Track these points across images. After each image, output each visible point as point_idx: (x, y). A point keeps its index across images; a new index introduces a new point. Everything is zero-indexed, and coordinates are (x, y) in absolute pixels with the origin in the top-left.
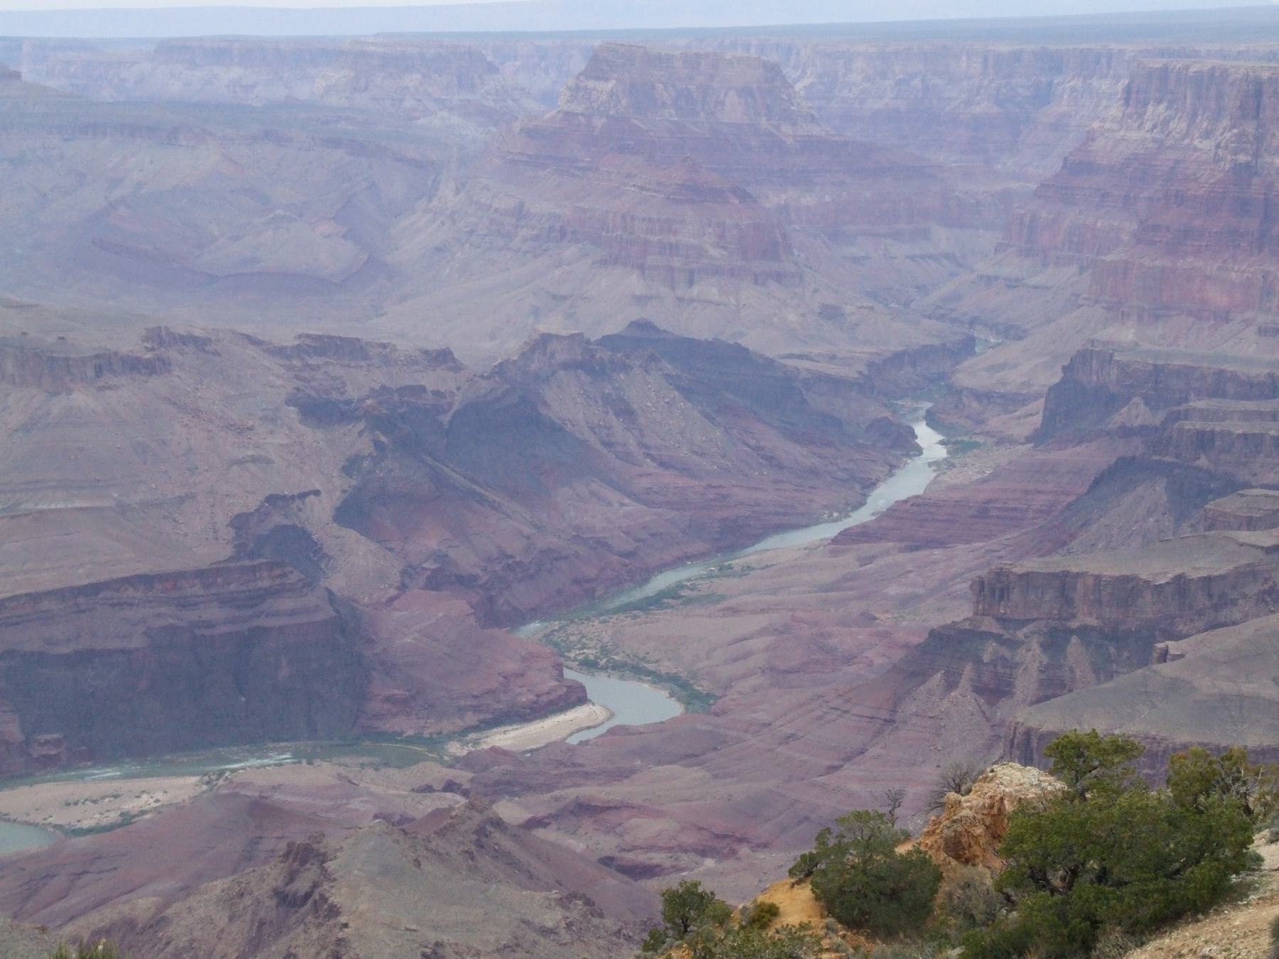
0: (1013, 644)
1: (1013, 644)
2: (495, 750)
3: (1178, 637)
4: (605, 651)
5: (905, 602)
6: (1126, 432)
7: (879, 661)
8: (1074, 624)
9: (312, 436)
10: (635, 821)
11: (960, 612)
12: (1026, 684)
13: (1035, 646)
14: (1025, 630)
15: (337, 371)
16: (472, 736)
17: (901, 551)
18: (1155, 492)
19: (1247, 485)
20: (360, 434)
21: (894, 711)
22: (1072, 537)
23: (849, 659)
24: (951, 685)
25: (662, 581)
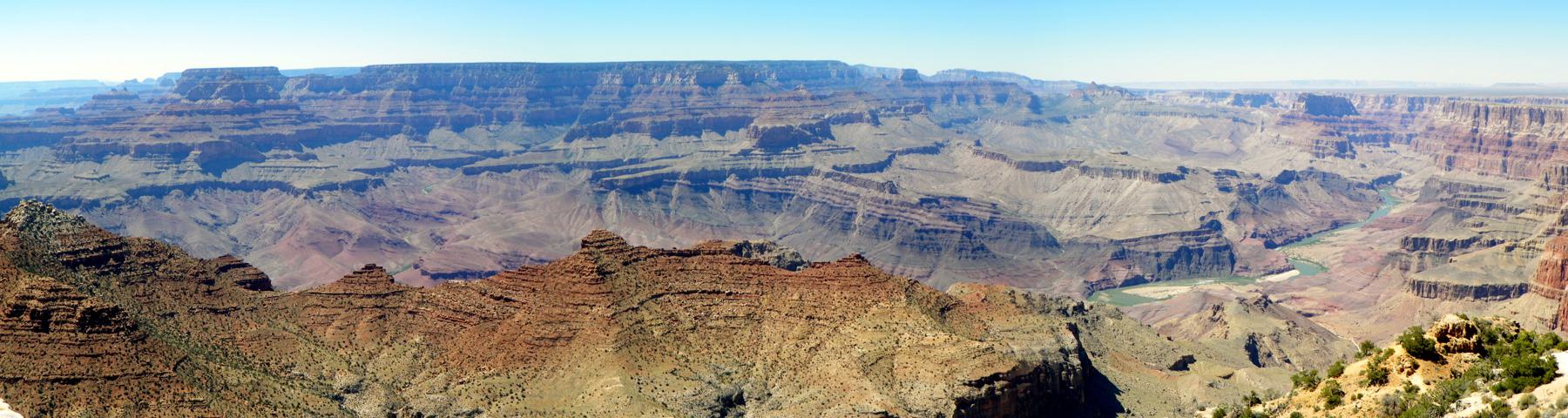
9: (1222, 195)
11: (1396, 248)
12: (1414, 268)
18: (1450, 216)
25: (1314, 237)
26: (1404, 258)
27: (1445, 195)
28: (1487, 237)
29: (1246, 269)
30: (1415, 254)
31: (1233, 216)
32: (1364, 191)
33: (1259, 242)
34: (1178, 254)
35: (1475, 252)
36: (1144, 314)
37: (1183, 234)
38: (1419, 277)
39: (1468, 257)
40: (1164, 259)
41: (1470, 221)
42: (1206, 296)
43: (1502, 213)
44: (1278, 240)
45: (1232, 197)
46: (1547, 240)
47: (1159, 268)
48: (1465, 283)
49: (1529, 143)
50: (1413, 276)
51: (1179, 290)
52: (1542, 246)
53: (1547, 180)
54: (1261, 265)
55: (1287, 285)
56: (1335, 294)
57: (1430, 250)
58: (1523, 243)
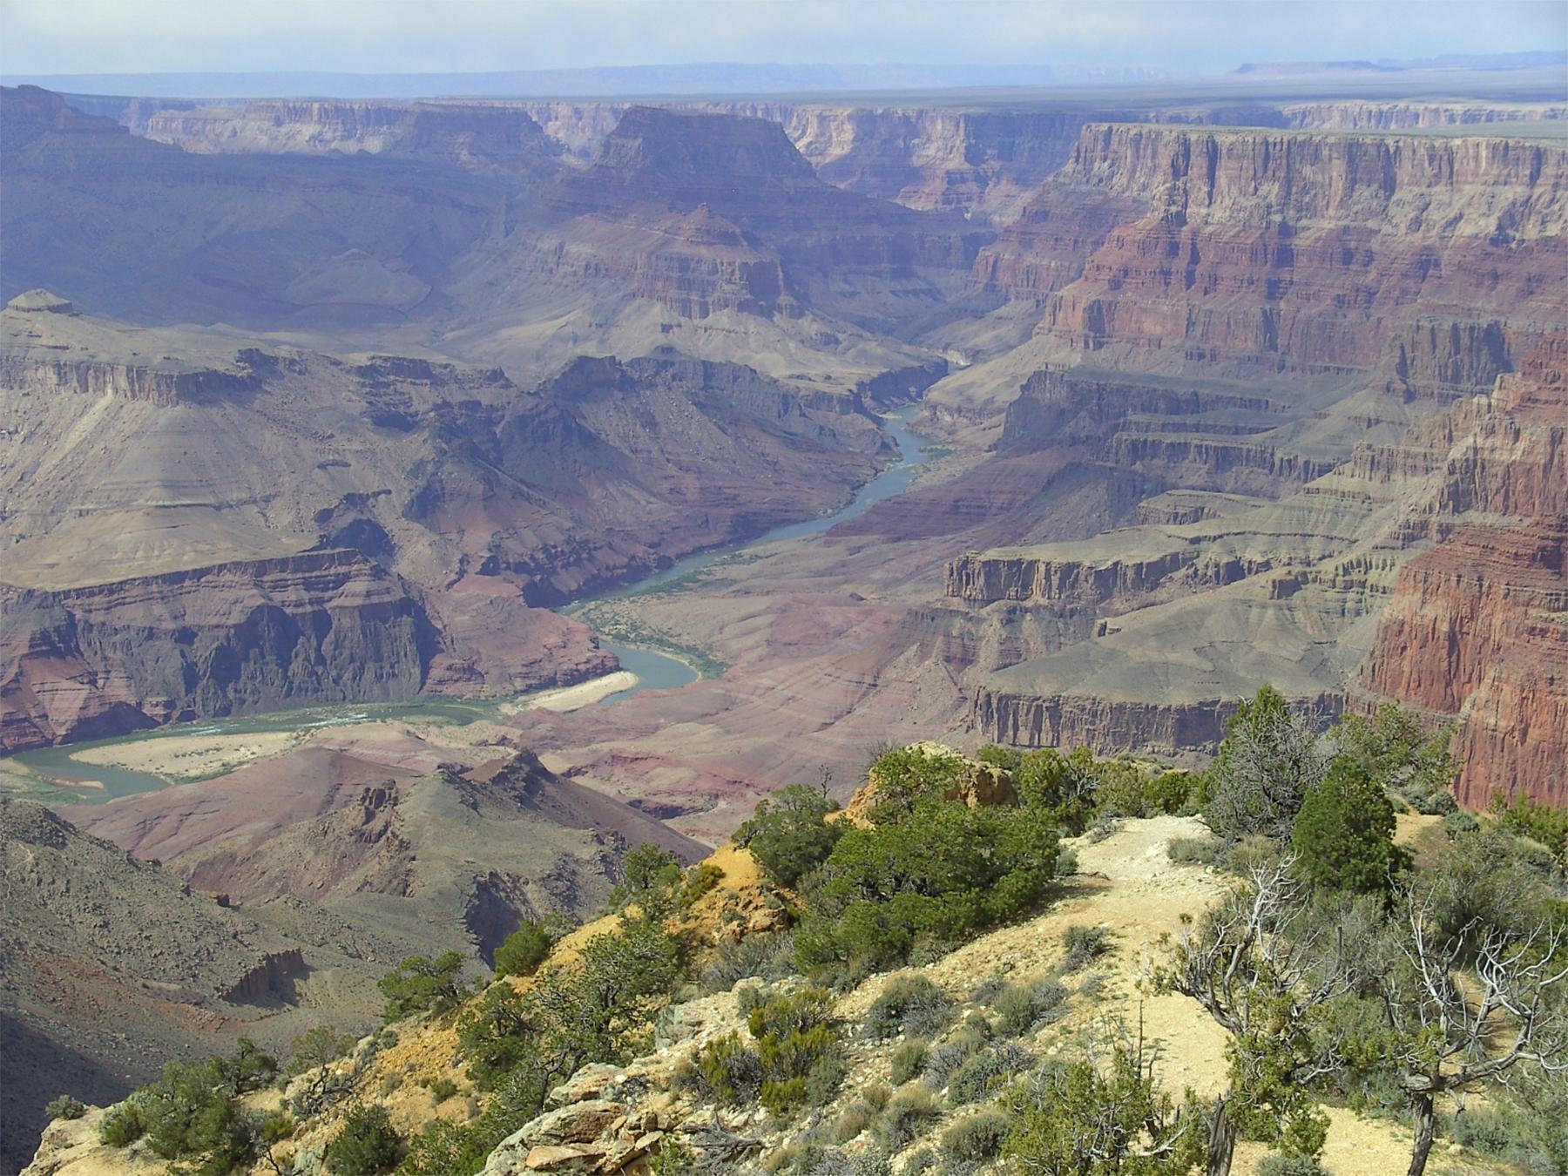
0: (979, 621)
1: (979, 621)
2: (541, 710)
3: (1117, 614)
4: (634, 627)
5: (886, 585)
6: (1074, 441)
7: (865, 635)
8: (1029, 604)
9: (383, 443)
10: (659, 770)
11: (934, 596)
12: (987, 654)
13: (996, 623)
14: (988, 608)
15: (406, 387)
16: (522, 698)
17: (884, 542)
19: (1175, 487)
20: (425, 441)
21: (876, 677)
22: (1029, 529)
23: (839, 634)
24: (923, 655)
25: (683, 568)
26: (958, 625)
27: (1083, 425)
28: (1214, 554)
29: (470, 672)
30: (992, 615)
31: (425, 506)
32: (832, 418)
33: (507, 589)
34: (248, 631)
35: (1176, 600)
36: (145, 827)
37: (262, 567)
38: (1003, 684)
39: (1157, 615)
40: (203, 650)
41: (1161, 503)
42: (340, 761)
43: (1261, 480)
44: (568, 581)
45: (418, 446)
46: (1402, 559)
47: (190, 676)
48: (1146, 699)
49: (1347, 251)
50: (983, 677)
51: (257, 747)
52: (1389, 578)
53: (1403, 369)
54: (515, 661)
55: (596, 722)
56: (748, 744)
57: (1037, 598)
58: (1328, 567)
